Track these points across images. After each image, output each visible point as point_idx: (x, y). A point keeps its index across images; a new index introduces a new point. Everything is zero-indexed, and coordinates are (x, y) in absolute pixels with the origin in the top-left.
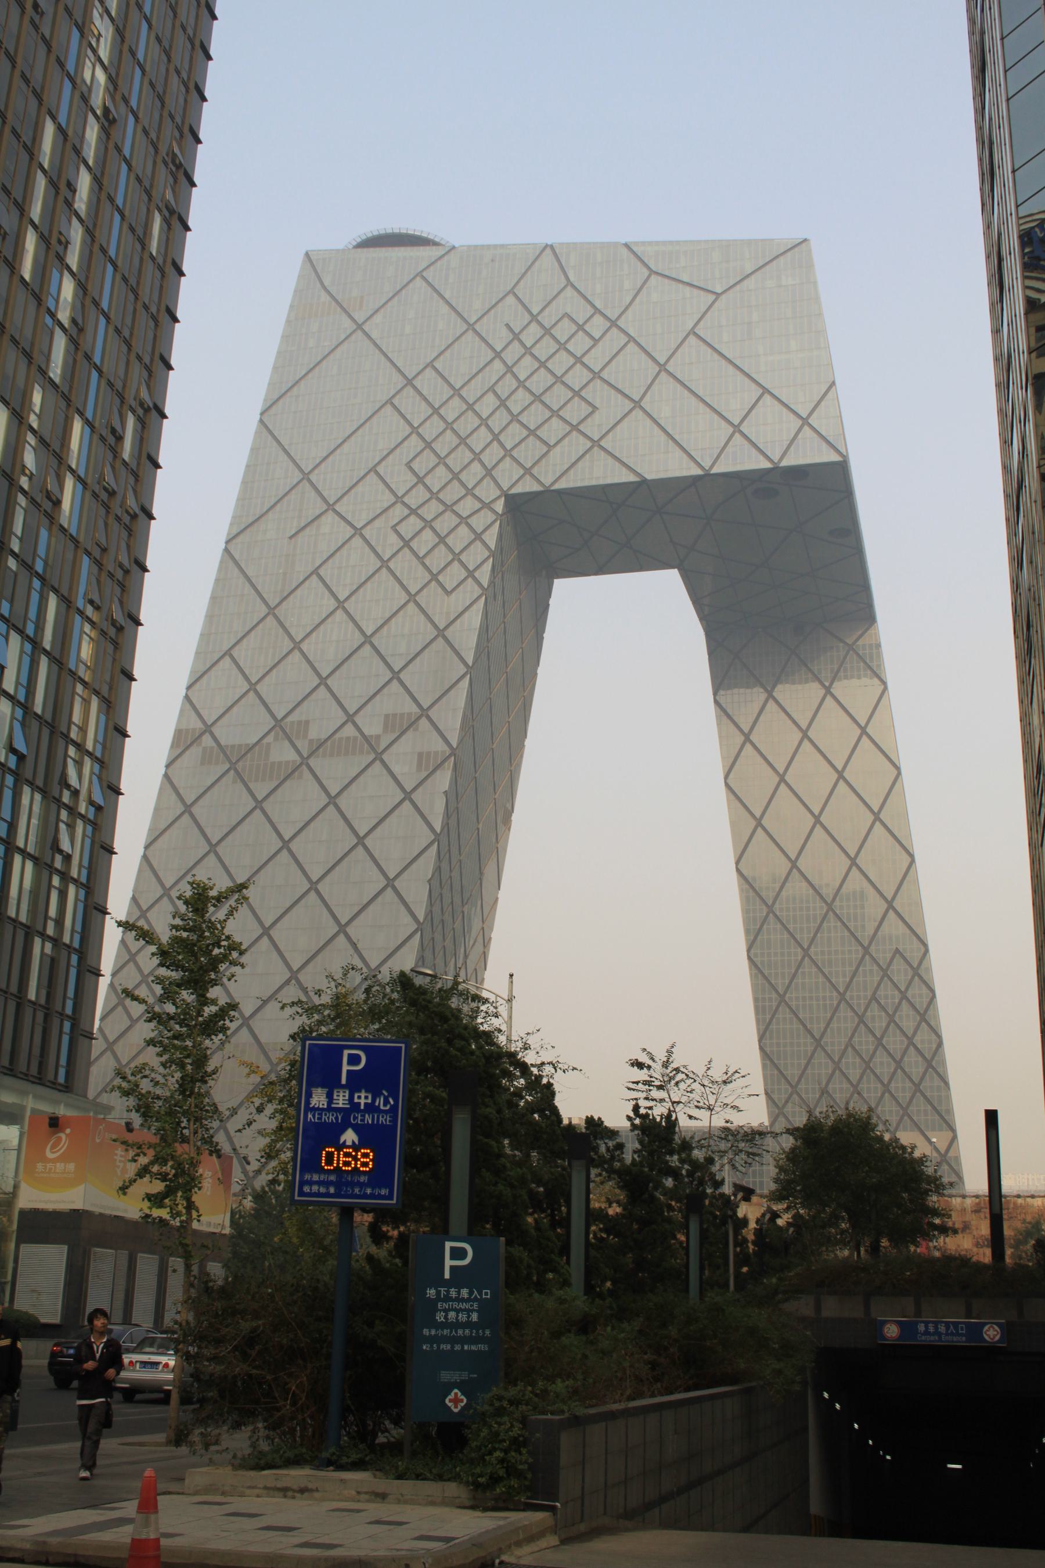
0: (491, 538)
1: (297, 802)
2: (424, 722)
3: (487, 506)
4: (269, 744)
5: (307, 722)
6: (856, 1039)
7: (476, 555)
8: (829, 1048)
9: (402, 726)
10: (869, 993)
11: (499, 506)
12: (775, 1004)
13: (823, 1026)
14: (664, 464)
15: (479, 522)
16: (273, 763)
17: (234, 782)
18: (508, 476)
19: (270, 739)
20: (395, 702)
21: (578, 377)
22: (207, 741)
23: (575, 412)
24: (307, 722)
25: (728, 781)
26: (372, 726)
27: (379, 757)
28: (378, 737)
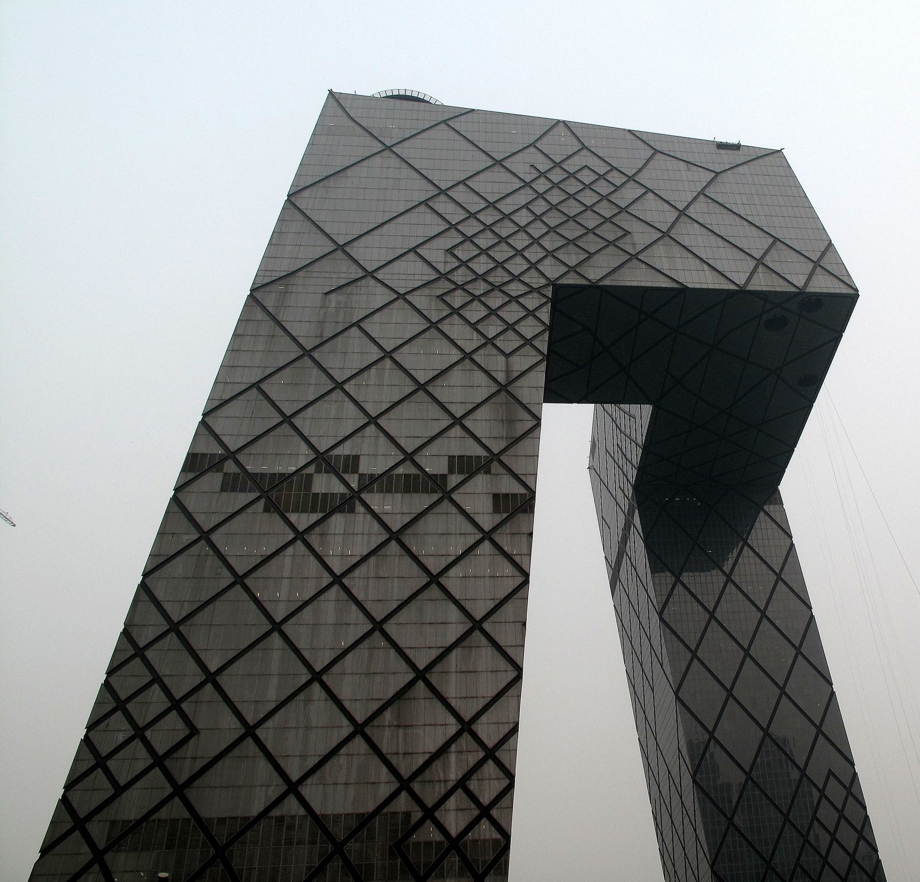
0: (545, 315)
1: (347, 538)
2: (495, 467)
3: (538, 290)
4: (310, 476)
5: (356, 458)
6: (803, 858)
7: (529, 329)
8: (779, 870)
9: (468, 467)
10: (810, 814)
11: (549, 292)
12: (724, 827)
13: (771, 847)
14: (697, 278)
15: (531, 302)
16: (316, 495)
17: (266, 510)
18: (552, 270)
19: (311, 470)
20: (457, 445)
21: (606, 210)
22: (230, 467)
23: (609, 233)
24: (356, 458)
25: (666, 617)
26: (434, 463)
27: (447, 496)
28: (444, 477)
